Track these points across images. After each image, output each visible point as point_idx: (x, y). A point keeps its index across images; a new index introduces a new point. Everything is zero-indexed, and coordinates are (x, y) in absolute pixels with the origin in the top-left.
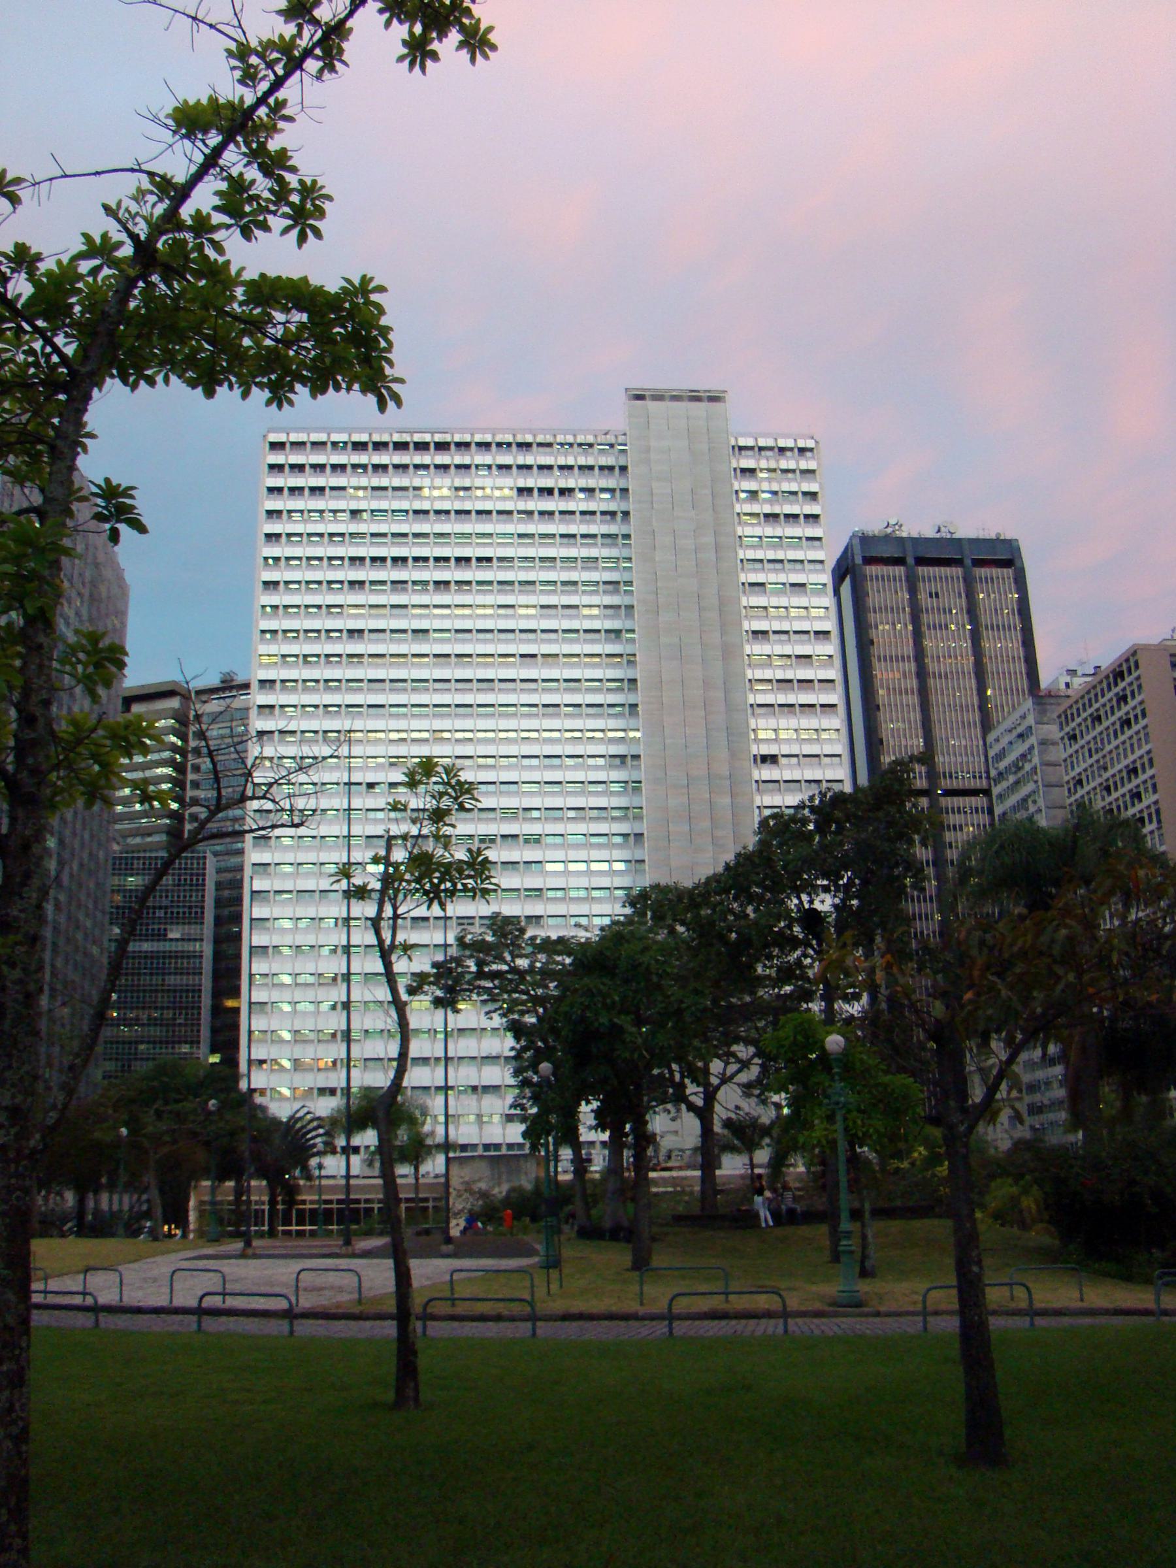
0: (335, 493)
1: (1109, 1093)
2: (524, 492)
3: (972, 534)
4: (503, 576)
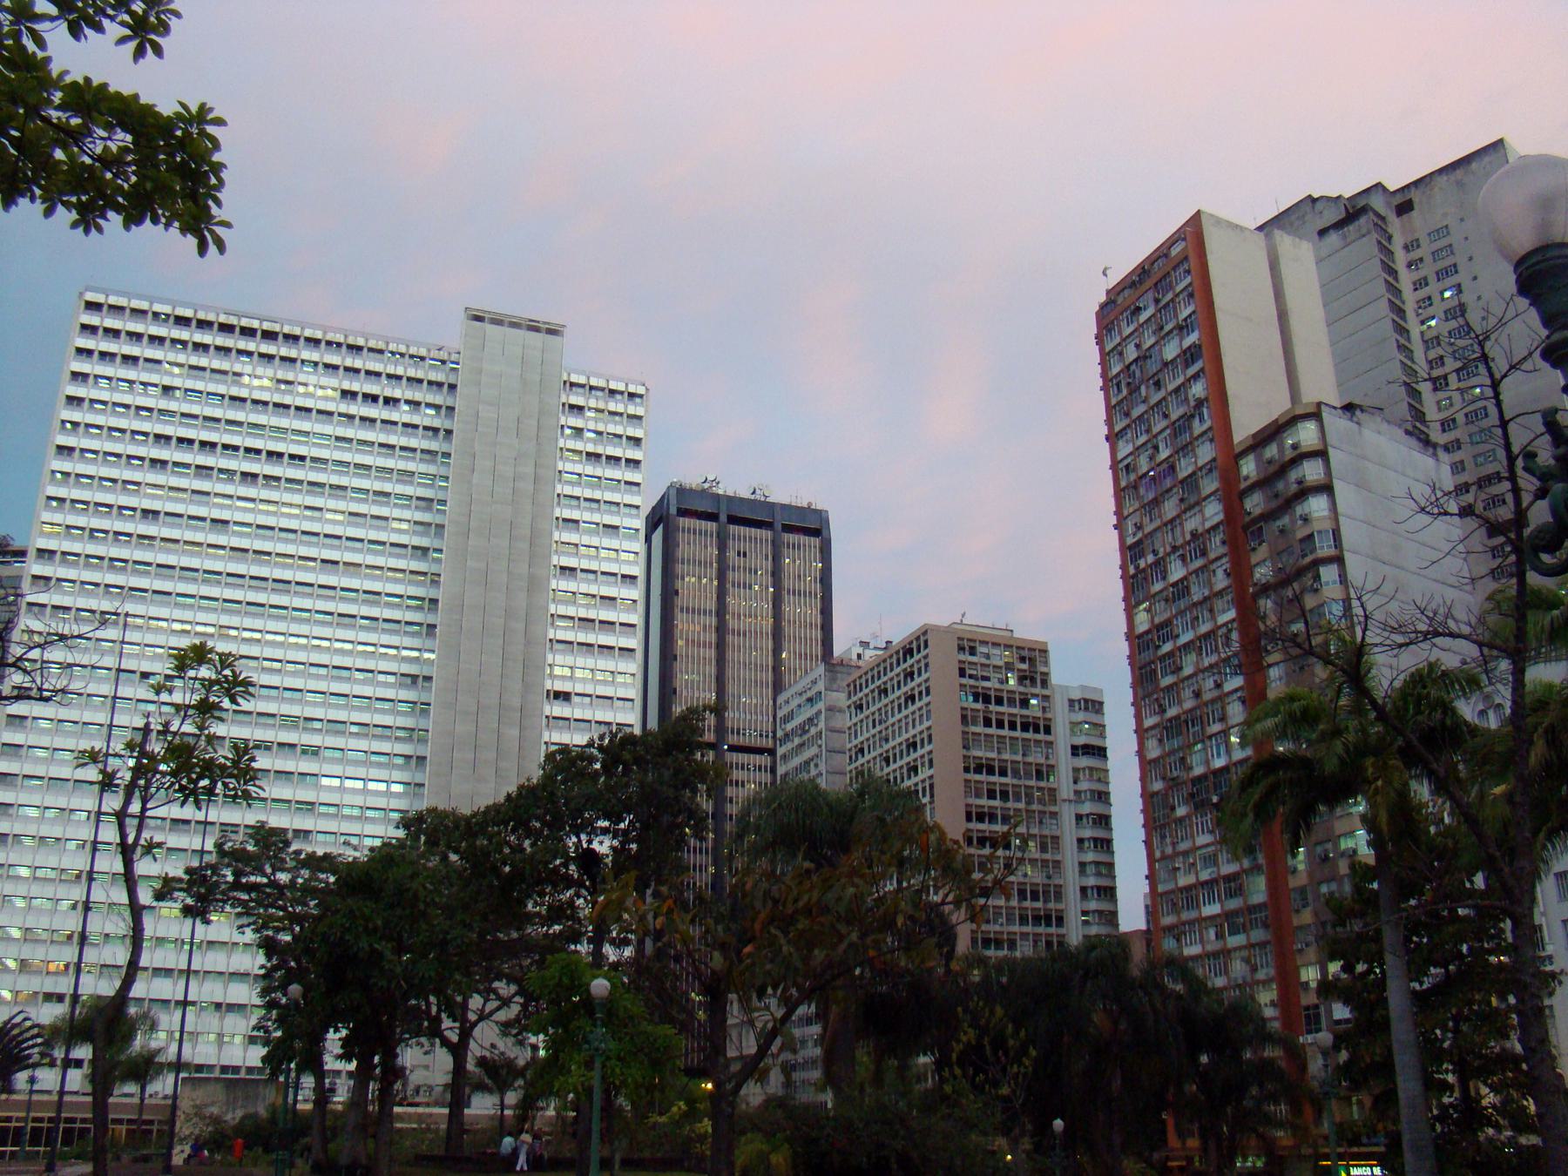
0: (149, 365)
1: (863, 1057)
2: (348, 395)
3: (785, 500)
4: (314, 476)
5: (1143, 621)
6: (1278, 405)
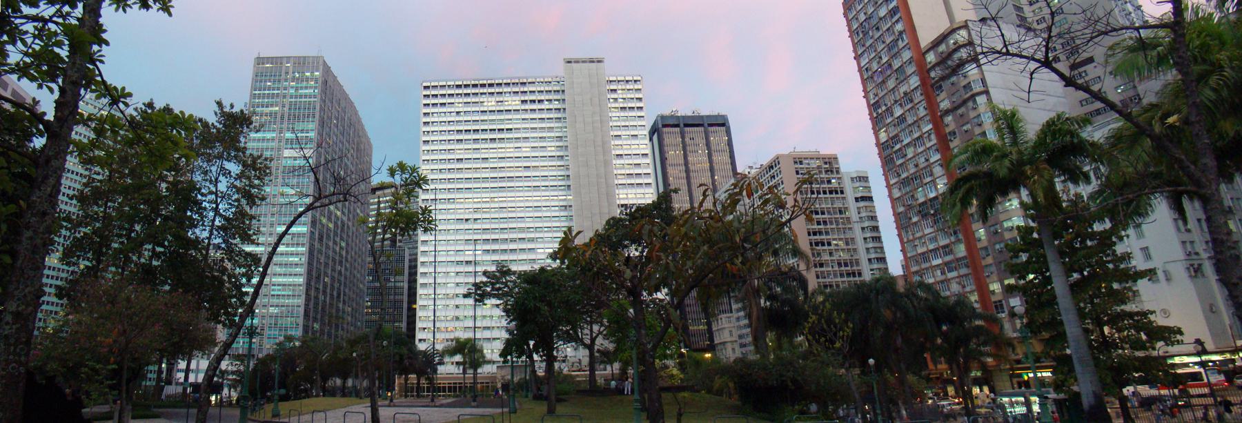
1: (770, 338)
2: (524, 102)
5: (883, 136)
6: (944, 25)
